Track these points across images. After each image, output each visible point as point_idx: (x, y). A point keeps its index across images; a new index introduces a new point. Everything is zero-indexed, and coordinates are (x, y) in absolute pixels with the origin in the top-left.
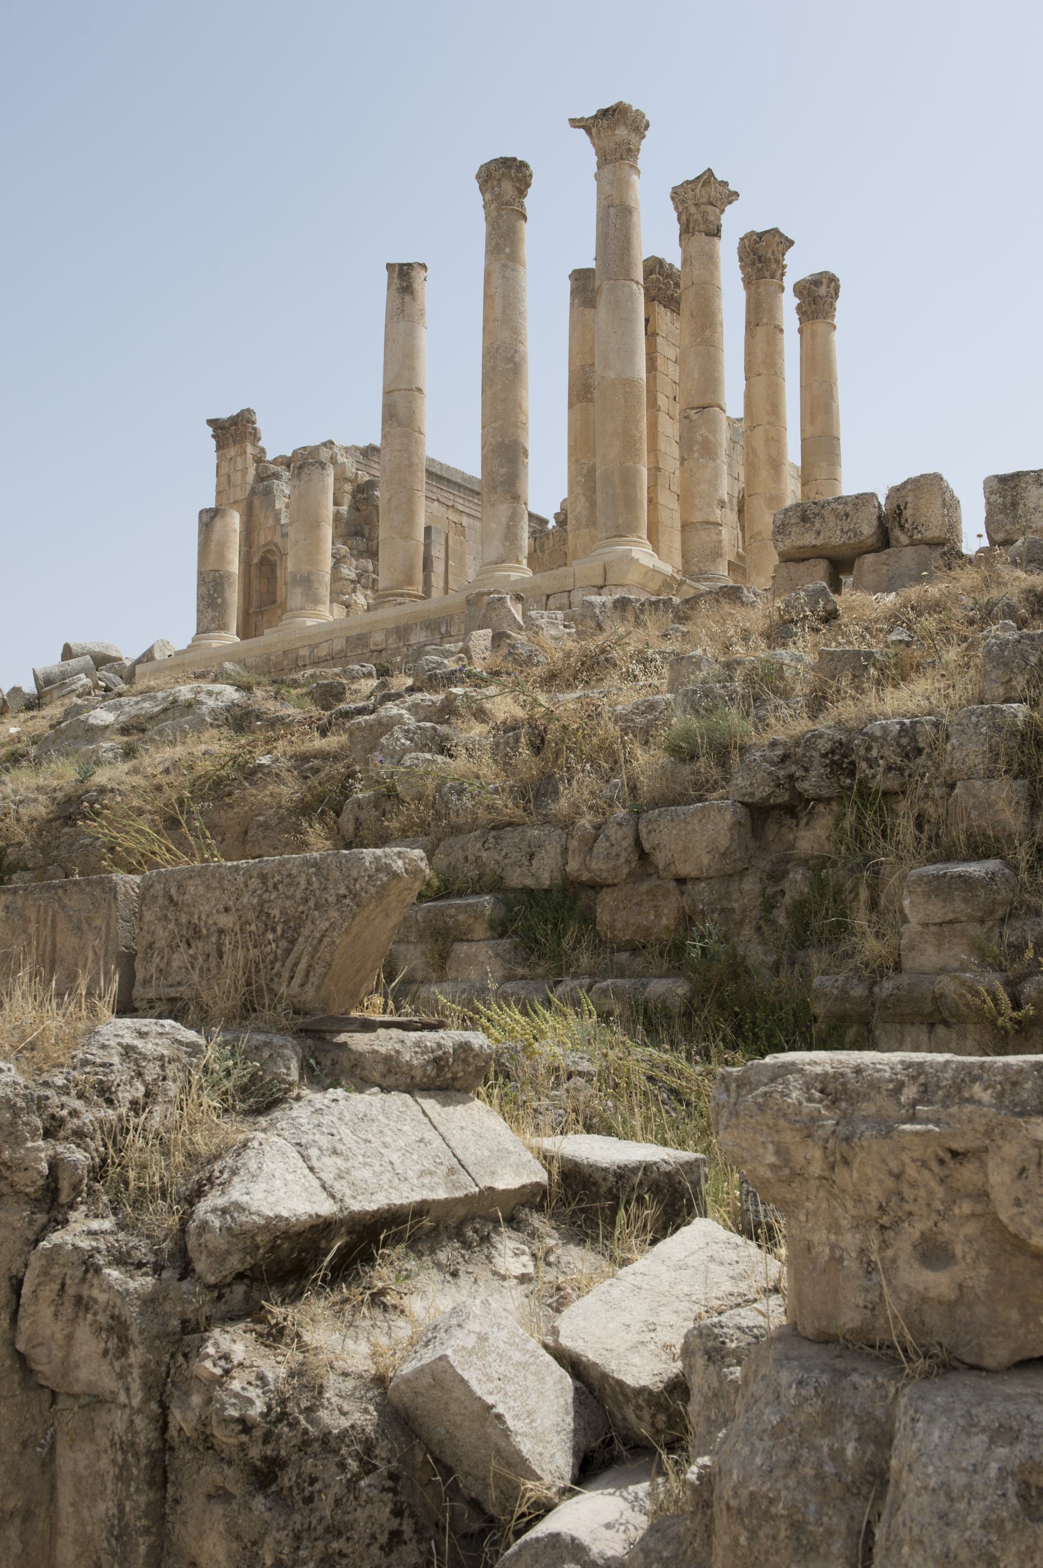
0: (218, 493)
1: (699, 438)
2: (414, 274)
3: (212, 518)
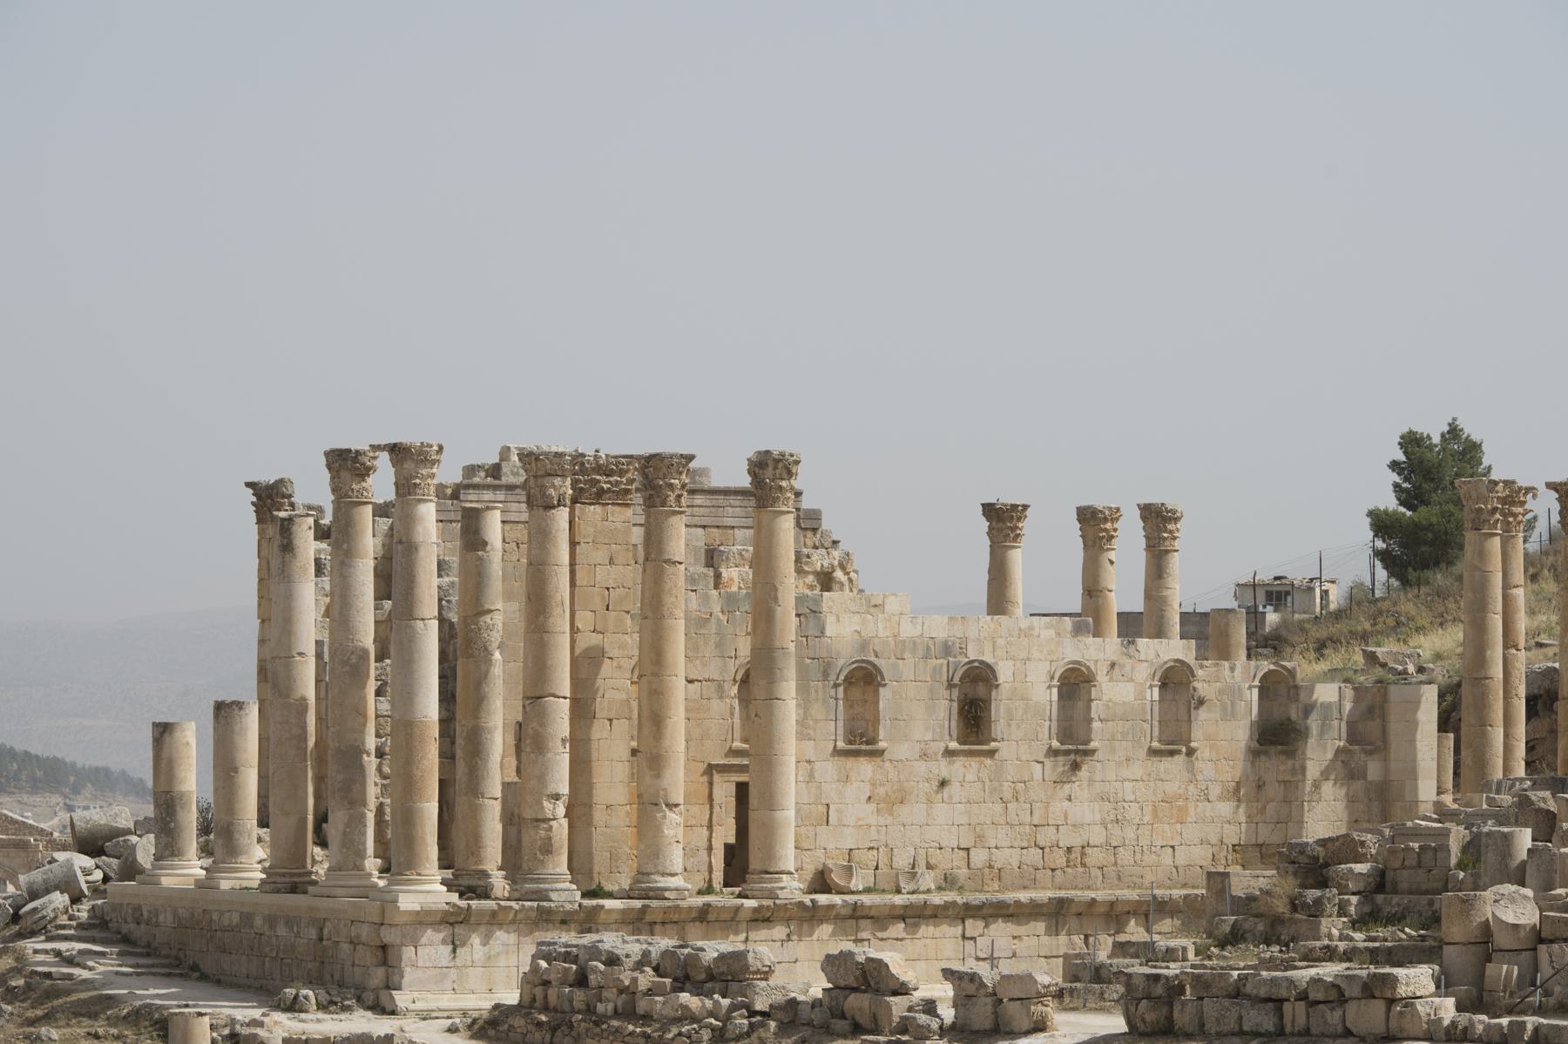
0: (261, 580)
1: (531, 732)
2: (295, 528)
3: (162, 734)
